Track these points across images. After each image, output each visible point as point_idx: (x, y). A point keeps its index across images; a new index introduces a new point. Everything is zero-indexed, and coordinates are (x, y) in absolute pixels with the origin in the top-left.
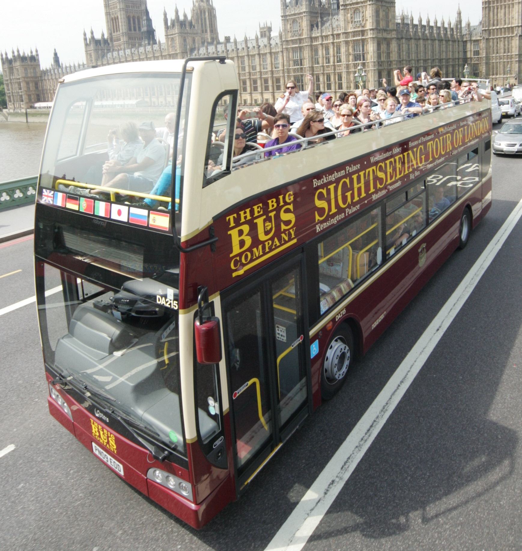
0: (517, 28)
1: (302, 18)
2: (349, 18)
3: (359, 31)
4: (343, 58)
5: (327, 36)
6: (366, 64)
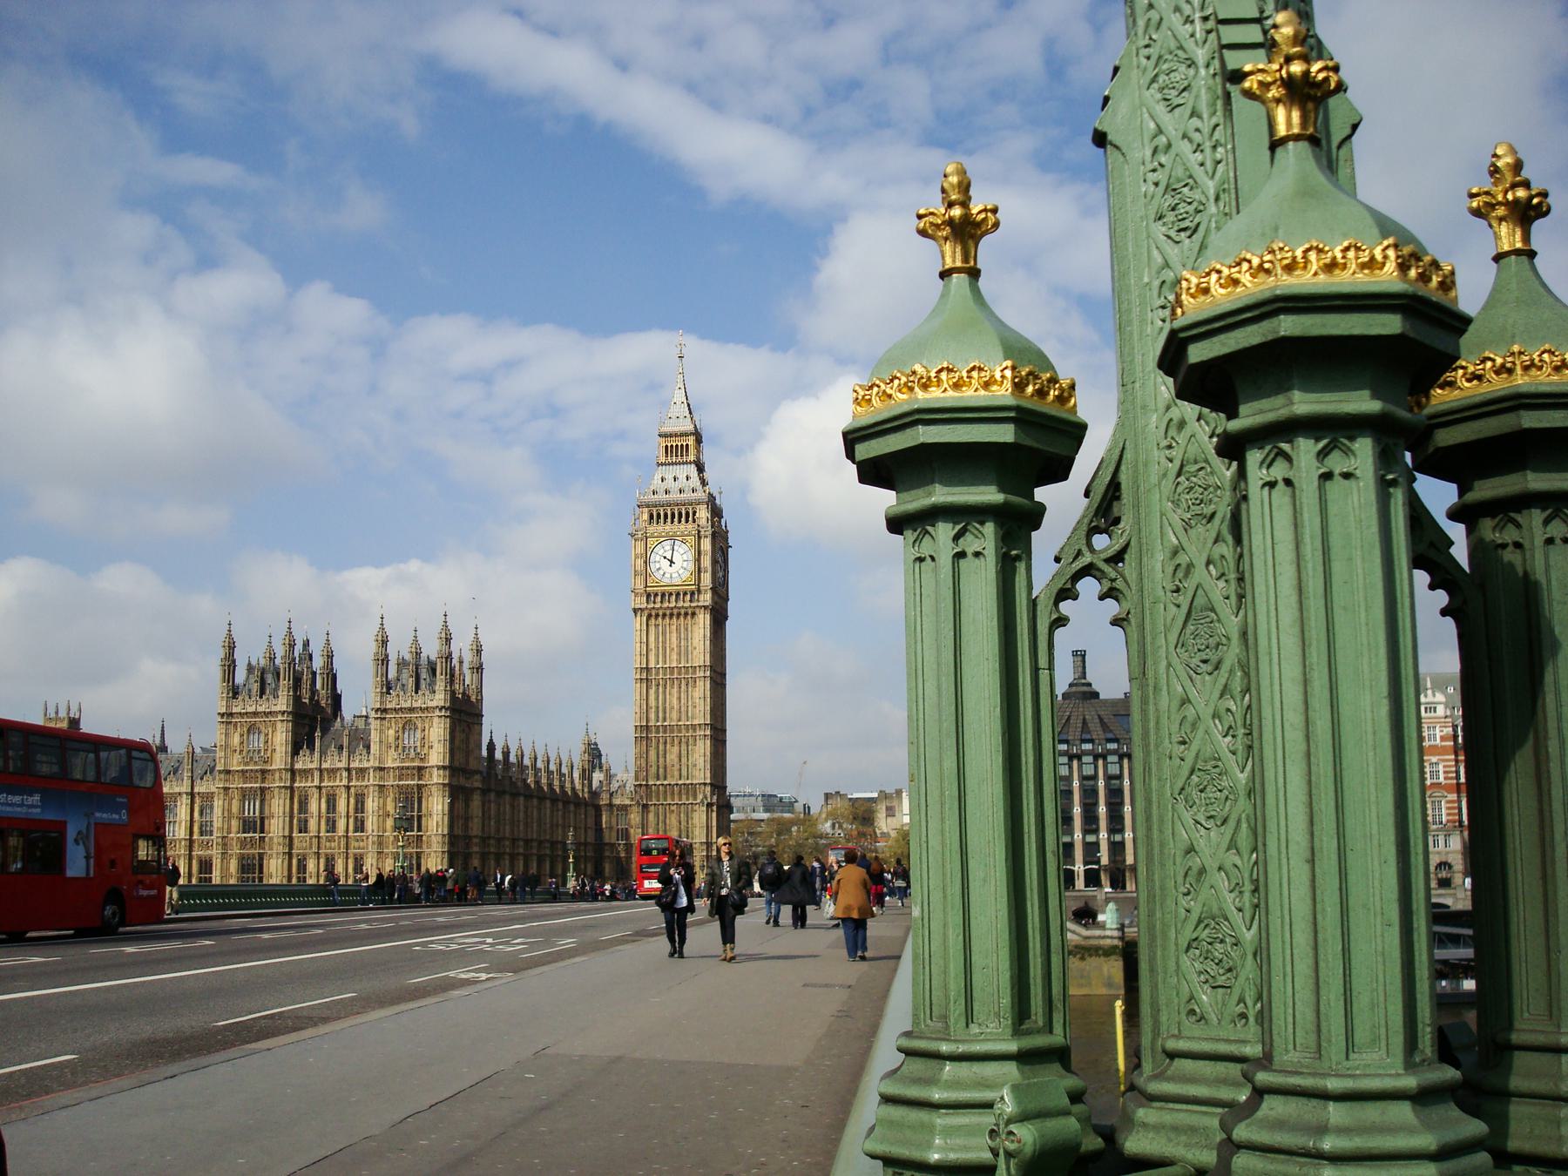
0: (703, 787)
1: (274, 724)
2: (391, 740)
3: (414, 768)
4: (371, 824)
5: (333, 772)
6: (424, 838)
